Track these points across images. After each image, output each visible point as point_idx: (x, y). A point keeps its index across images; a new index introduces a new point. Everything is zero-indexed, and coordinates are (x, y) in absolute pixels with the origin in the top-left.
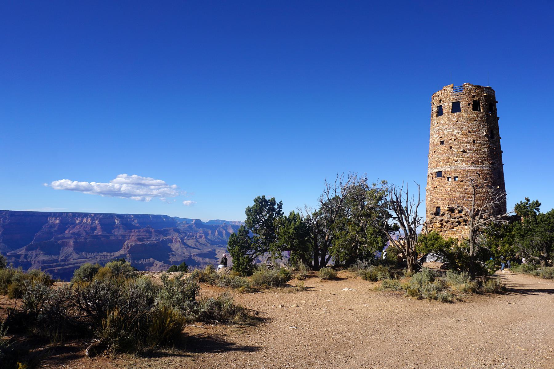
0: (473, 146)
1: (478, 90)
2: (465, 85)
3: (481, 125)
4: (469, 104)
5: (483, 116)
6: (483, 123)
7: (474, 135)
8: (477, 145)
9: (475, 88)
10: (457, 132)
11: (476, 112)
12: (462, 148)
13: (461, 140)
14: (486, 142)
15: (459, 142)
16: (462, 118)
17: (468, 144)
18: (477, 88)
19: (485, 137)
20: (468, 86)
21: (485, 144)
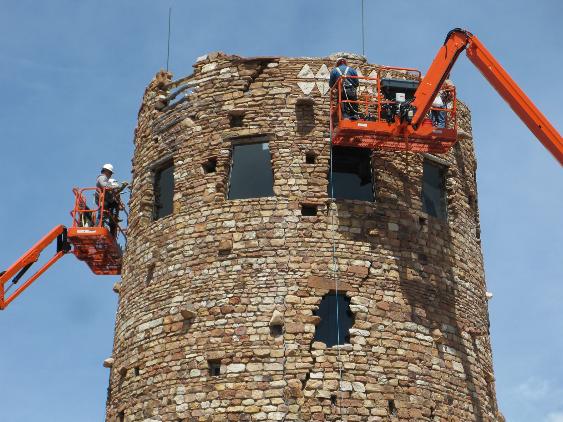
0: (203, 395)
1: (263, 80)
2: (203, 63)
3: (259, 271)
4: (210, 166)
5: (280, 218)
6: (270, 260)
7: (214, 332)
8: (222, 387)
9: (249, 72)
10: (146, 326)
11: (237, 202)
12: (155, 412)
13: (156, 370)
14: (279, 367)
15: (149, 383)
16: (171, 246)
17: (182, 389)
18: (260, 72)
19: (280, 339)
20: (212, 66)
21: (270, 378)
